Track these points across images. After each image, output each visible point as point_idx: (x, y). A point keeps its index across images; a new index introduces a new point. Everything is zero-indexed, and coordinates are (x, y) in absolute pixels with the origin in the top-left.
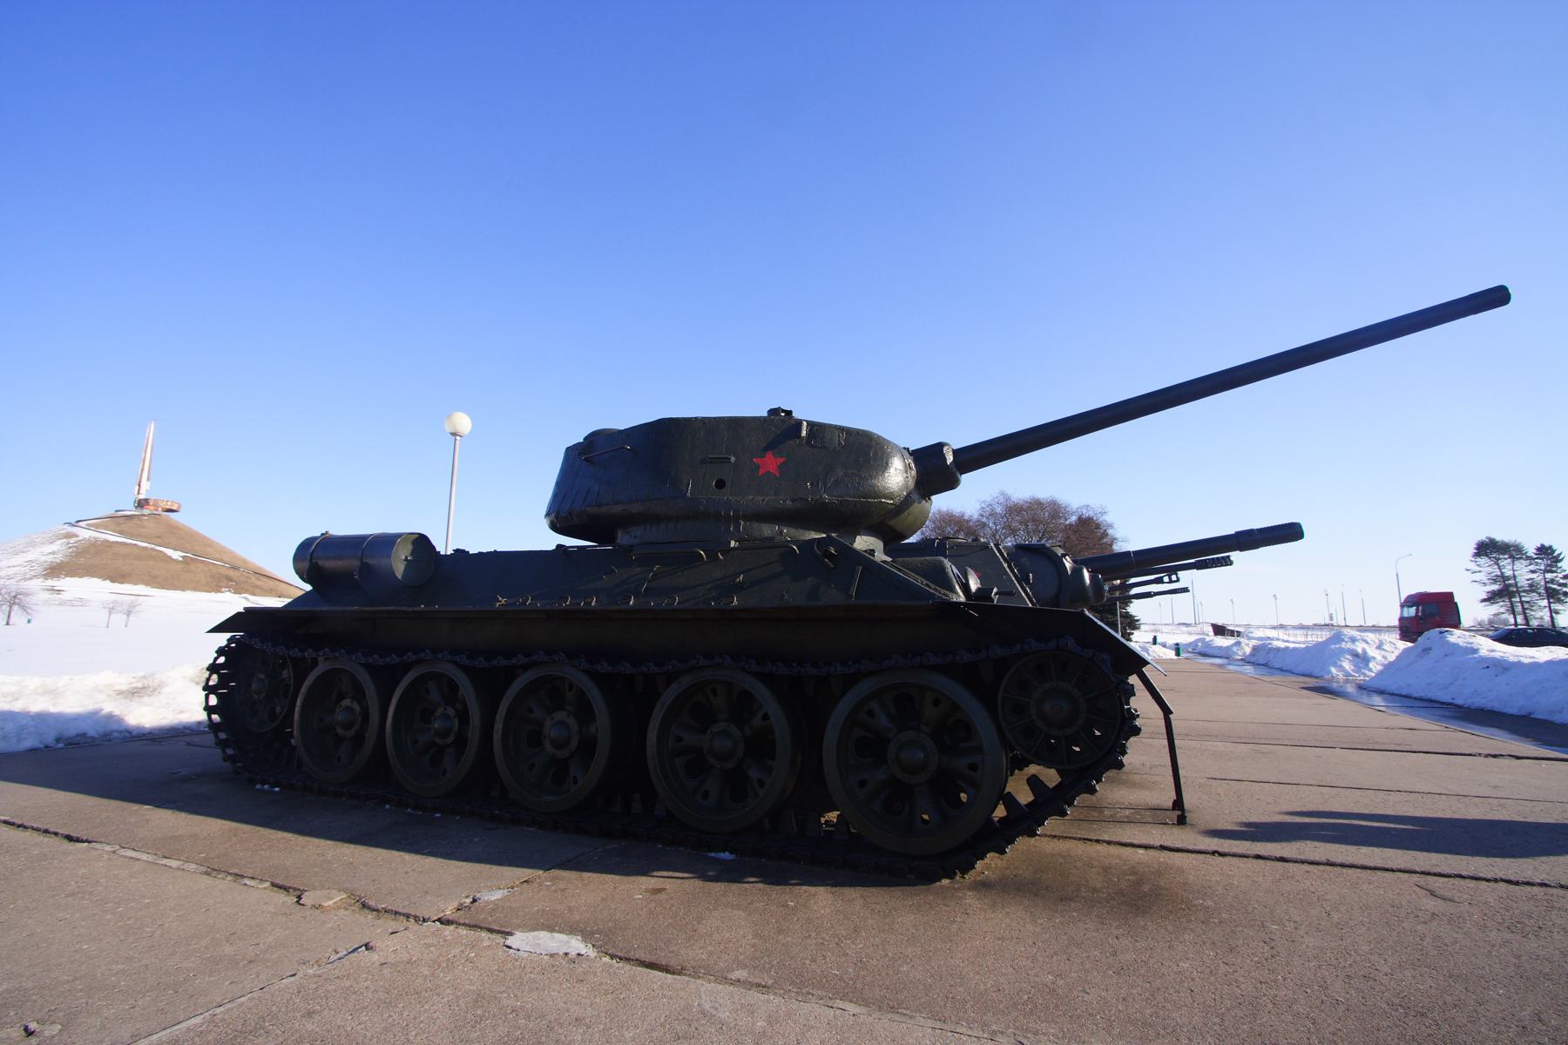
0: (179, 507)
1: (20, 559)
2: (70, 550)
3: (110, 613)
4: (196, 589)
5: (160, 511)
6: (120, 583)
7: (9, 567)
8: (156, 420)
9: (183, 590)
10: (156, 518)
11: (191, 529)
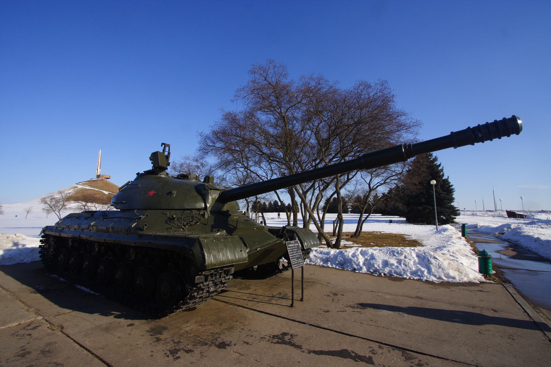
0: (110, 177)
3: (28, 213)
8: (101, 148)
11: (114, 184)
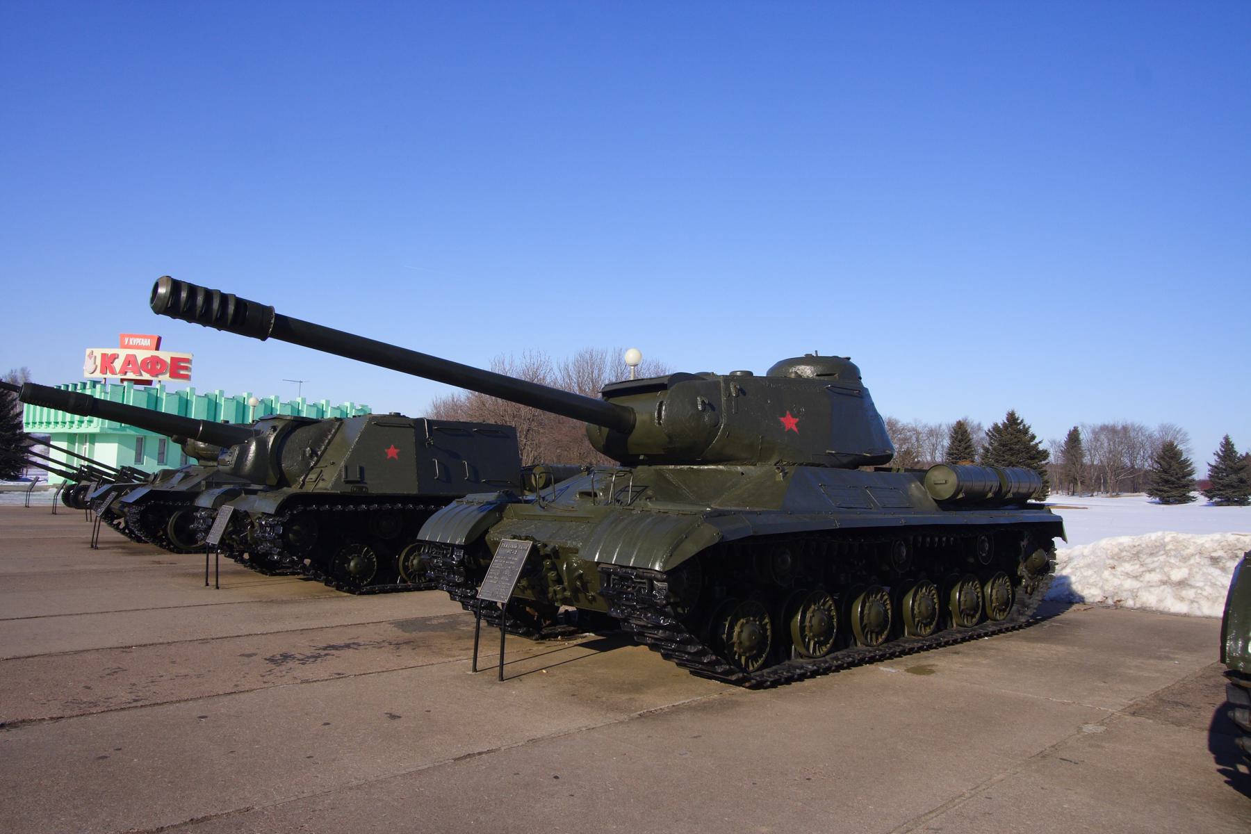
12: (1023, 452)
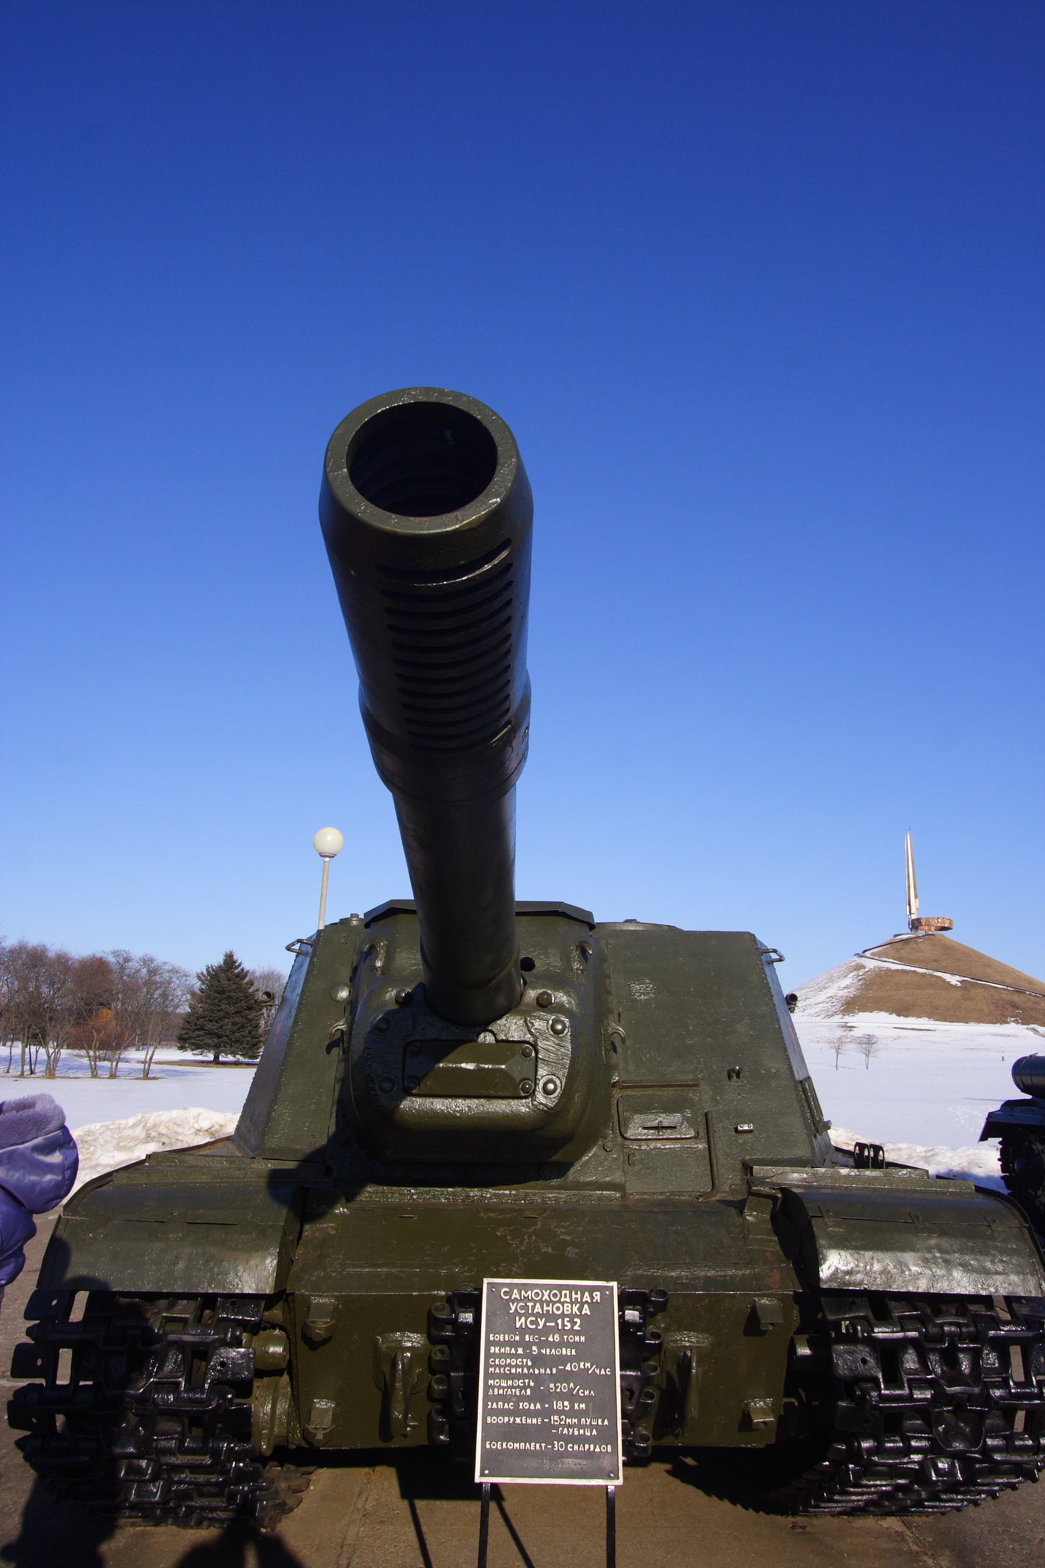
0: (951, 923)
1: (823, 996)
2: (860, 983)
3: (838, 1051)
4: (979, 1020)
5: (933, 931)
6: (905, 1016)
7: (816, 1004)
9: (967, 1023)
10: (931, 940)
12: (241, 1001)
